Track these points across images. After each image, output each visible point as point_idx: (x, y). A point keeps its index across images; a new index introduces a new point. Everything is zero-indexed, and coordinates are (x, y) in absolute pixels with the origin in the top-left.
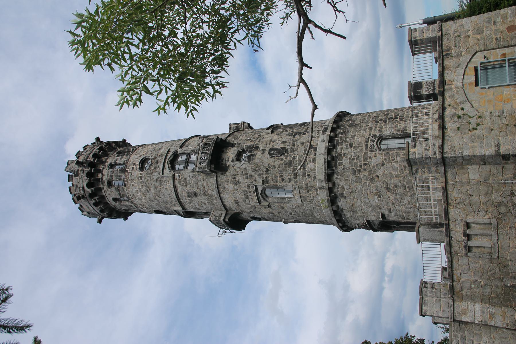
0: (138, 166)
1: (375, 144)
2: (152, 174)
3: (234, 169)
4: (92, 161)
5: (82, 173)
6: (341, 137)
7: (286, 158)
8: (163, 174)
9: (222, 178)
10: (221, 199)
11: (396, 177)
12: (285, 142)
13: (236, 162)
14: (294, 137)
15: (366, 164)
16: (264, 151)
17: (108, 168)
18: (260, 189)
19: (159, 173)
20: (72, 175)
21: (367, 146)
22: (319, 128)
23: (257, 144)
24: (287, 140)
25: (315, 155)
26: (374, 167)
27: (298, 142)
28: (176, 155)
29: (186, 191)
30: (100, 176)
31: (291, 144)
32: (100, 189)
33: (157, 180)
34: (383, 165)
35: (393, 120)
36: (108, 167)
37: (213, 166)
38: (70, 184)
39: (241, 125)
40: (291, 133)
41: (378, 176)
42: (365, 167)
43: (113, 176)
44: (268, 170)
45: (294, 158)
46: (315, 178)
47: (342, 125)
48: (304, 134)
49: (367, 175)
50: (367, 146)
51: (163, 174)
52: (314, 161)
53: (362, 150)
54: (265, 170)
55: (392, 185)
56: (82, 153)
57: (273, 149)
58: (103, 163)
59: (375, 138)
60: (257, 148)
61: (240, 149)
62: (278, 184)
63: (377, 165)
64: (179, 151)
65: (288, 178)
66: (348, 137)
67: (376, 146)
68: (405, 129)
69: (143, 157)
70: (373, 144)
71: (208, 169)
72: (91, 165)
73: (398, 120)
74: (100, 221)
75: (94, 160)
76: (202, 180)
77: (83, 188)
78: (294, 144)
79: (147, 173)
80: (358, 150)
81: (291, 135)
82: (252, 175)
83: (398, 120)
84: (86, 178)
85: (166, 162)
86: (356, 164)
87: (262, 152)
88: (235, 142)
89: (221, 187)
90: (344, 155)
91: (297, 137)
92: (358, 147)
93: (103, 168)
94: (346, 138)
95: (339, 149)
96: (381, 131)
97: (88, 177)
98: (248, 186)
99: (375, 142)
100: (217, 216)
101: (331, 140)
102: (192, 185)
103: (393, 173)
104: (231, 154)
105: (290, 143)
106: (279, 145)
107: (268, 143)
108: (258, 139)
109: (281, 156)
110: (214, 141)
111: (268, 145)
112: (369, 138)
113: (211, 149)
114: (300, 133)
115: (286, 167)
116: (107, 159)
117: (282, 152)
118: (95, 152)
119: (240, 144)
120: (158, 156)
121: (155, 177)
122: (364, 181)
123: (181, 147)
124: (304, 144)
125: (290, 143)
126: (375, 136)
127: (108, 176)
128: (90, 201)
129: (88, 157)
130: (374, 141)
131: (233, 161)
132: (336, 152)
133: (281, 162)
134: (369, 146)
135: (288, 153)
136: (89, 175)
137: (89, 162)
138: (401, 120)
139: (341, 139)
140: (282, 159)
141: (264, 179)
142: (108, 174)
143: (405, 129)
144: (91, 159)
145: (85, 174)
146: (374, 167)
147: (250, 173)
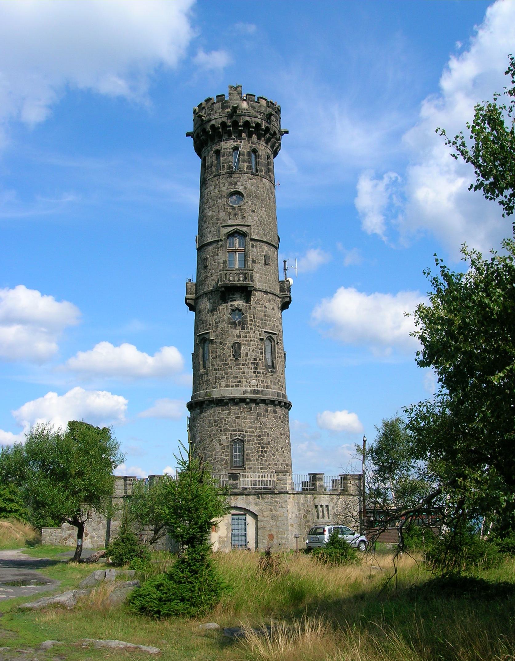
0: (233, 190)
1: (236, 437)
2: (224, 211)
3: (224, 309)
4: (239, 124)
5: (225, 114)
6: (246, 408)
7: (231, 360)
8: (223, 227)
9: (217, 297)
10: (202, 295)
11: (211, 455)
12: (247, 356)
13: (230, 310)
14: (252, 363)
15: (221, 431)
16: (239, 336)
17: (233, 146)
18: (206, 336)
19: (224, 221)
20: (224, 99)
21: (236, 431)
22: (262, 384)
23: (247, 327)
24: (249, 357)
25: (232, 387)
26: (219, 437)
27: (246, 370)
28: (244, 235)
29: (208, 256)
30: (226, 137)
31: (244, 362)
32: (212, 140)
33: (218, 219)
34: (220, 445)
35: (261, 449)
36: (235, 146)
37: (224, 289)
38: (215, 100)
39: (285, 294)
40: (258, 359)
41: (212, 441)
42: (219, 431)
43: (225, 157)
44: (221, 343)
45: (230, 367)
46: (214, 388)
47: (260, 406)
48: (254, 372)
49: (214, 432)
50: (236, 431)
51: (223, 227)
52: (227, 386)
53: (233, 427)
54: (222, 340)
55: (206, 452)
56: (251, 101)
57: (239, 345)
58: (240, 136)
59: (242, 437)
60: (243, 329)
61: (244, 311)
62: (211, 354)
63: (220, 440)
64: (248, 239)
65: (215, 363)
66: (245, 414)
67: (234, 438)
68: (249, 460)
69: (244, 194)
70: (237, 436)
71: (220, 285)
72: (235, 124)
73: (260, 454)
74: (188, 135)
75: (240, 126)
76: (216, 274)
77: (210, 120)
78: (244, 365)
79: (225, 204)
80: (233, 424)
81: (255, 360)
82: (218, 328)
83: (260, 454)
84: (220, 122)
85: (235, 227)
86: (221, 423)
87: (238, 334)
88: (252, 302)
89: (209, 296)
90: (229, 412)
91: (253, 366)
92: (235, 423)
93: (233, 139)
94: (244, 412)
95: (235, 407)
96: (249, 441)
97: (221, 124)
98: (210, 325)
99: (239, 438)
100: (191, 289)
101: (243, 400)
102: (213, 262)
103: (214, 452)
104: (239, 303)
105: (246, 361)
106: (243, 350)
107: (247, 339)
108: (254, 327)
109: (233, 355)
110: (249, 284)
111: (245, 339)
112: (243, 431)
113: (239, 284)
114: (256, 368)
115: (222, 360)
116: (245, 139)
117: (237, 355)
118: (252, 121)
119: (250, 308)
120: (243, 213)
121: (220, 216)
122: (210, 429)
123: (252, 240)
124: (243, 375)
125: (246, 361)
126: (244, 436)
127: (224, 149)
128: (199, 128)
129: (245, 115)
130: (239, 436)
131: (232, 305)
132: (231, 406)
133: (228, 355)
134: (236, 433)
135: (235, 361)
136: (224, 124)
137: (237, 120)
138: (259, 456)
139: (244, 408)
140: (230, 356)
141: (215, 341)
142: (226, 149)
143: (249, 460)
144: (241, 121)
145: (225, 119)
146: (219, 437)
147: (220, 326)
